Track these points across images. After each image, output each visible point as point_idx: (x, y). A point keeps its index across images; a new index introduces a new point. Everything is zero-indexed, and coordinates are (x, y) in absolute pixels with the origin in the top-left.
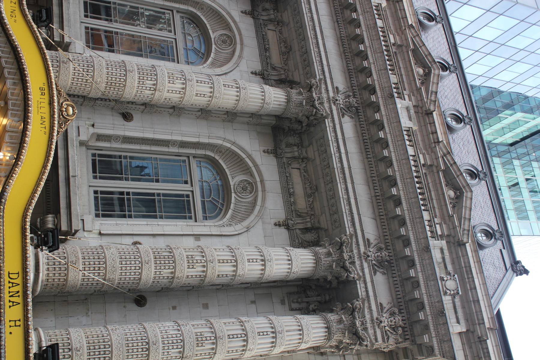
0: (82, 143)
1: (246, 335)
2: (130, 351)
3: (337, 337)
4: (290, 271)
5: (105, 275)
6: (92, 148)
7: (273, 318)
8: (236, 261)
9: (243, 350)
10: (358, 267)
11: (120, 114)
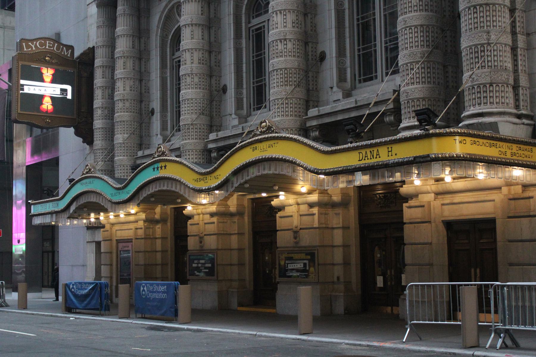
0: (347, 95)
2: (482, 25)
5: (417, 62)
6: (353, 85)
11: (321, 64)
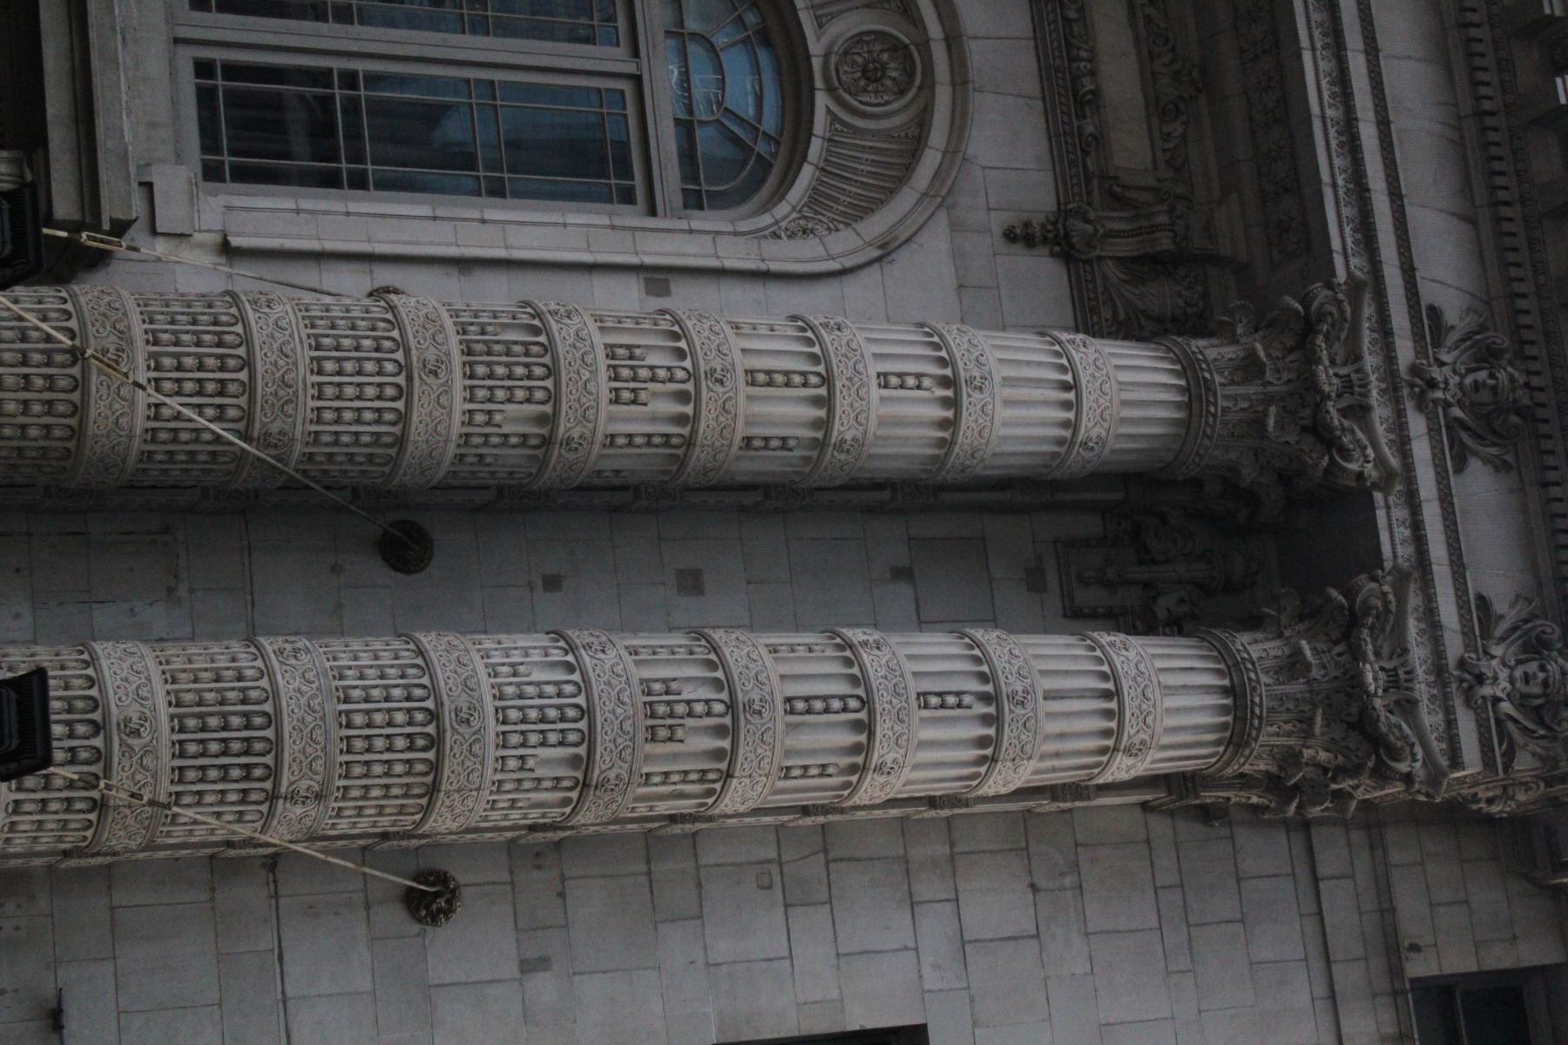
1: (866, 703)
3: (1272, 737)
4: (1067, 434)
5: (248, 415)
7: (988, 637)
8: (827, 380)
9: (853, 769)
10: (1380, 429)
